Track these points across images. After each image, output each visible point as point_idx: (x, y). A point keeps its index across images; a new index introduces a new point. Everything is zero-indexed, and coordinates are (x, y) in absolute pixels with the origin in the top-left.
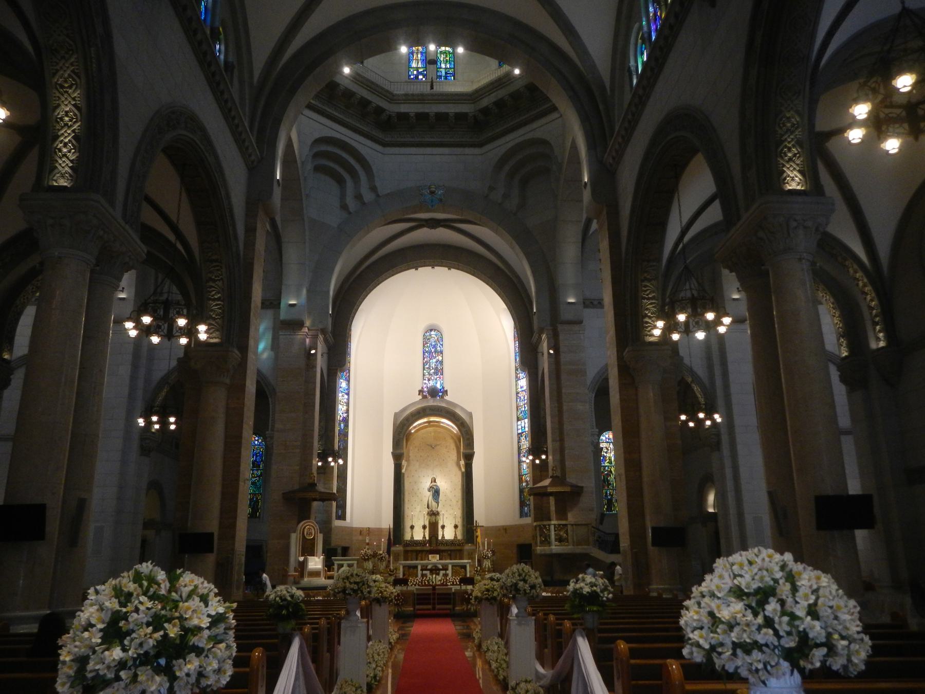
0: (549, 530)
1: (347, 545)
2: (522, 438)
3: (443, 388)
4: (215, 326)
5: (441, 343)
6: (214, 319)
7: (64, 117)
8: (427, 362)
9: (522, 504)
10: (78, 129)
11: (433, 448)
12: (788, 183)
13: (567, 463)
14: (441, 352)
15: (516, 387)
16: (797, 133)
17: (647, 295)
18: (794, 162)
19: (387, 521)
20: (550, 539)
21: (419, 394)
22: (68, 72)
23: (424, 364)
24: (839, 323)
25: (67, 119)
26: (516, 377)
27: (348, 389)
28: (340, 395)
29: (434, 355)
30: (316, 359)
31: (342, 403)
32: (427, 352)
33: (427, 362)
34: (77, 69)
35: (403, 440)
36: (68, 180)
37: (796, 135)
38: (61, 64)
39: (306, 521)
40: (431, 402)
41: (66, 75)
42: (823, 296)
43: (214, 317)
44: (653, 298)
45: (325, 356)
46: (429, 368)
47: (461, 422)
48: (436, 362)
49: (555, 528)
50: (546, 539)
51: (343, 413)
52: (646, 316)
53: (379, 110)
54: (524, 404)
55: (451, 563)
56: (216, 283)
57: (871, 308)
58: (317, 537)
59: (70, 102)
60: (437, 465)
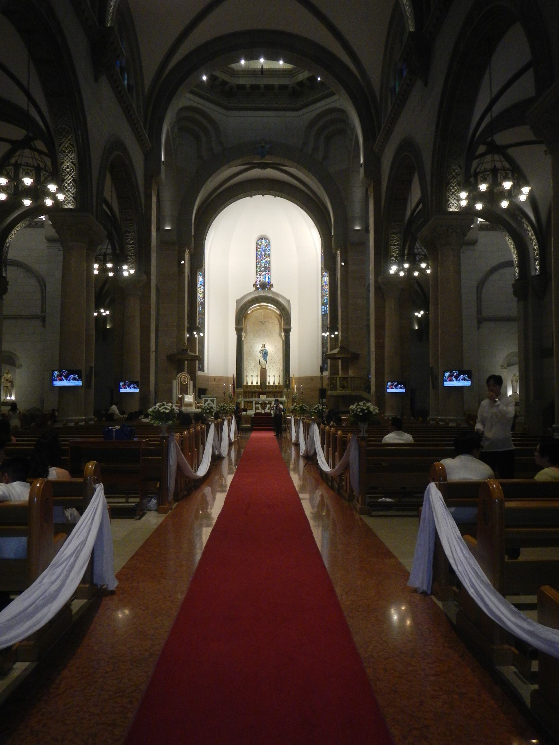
0: (336, 381)
1: (206, 388)
3: (271, 282)
4: (131, 260)
5: (269, 248)
6: (131, 256)
7: (67, 169)
8: (259, 262)
9: (324, 362)
10: (75, 176)
11: (263, 324)
12: (450, 207)
14: (269, 255)
15: (322, 282)
16: (458, 178)
17: (394, 243)
18: (455, 195)
19: (232, 372)
20: (337, 386)
21: (254, 287)
22: (68, 144)
23: (257, 264)
24: (516, 258)
25: (68, 170)
27: (204, 282)
28: (199, 286)
29: (264, 257)
30: (185, 267)
31: (200, 292)
34: (72, 142)
35: (243, 319)
36: (72, 204)
37: (458, 179)
38: (63, 140)
39: (181, 373)
40: (262, 293)
41: (66, 146)
42: (508, 240)
43: (131, 255)
44: (397, 245)
45: (189, 261)
46: (260, 267)
48: (266, 262)
49: (340, 380)
50: (334, 387)
51: (200, 299)
52: (393, 256)
53: (224, 83)
54: (327, 294)
56: (131, 233)
57: (534, 250)
58: (189, 383)
59: (69, 160)
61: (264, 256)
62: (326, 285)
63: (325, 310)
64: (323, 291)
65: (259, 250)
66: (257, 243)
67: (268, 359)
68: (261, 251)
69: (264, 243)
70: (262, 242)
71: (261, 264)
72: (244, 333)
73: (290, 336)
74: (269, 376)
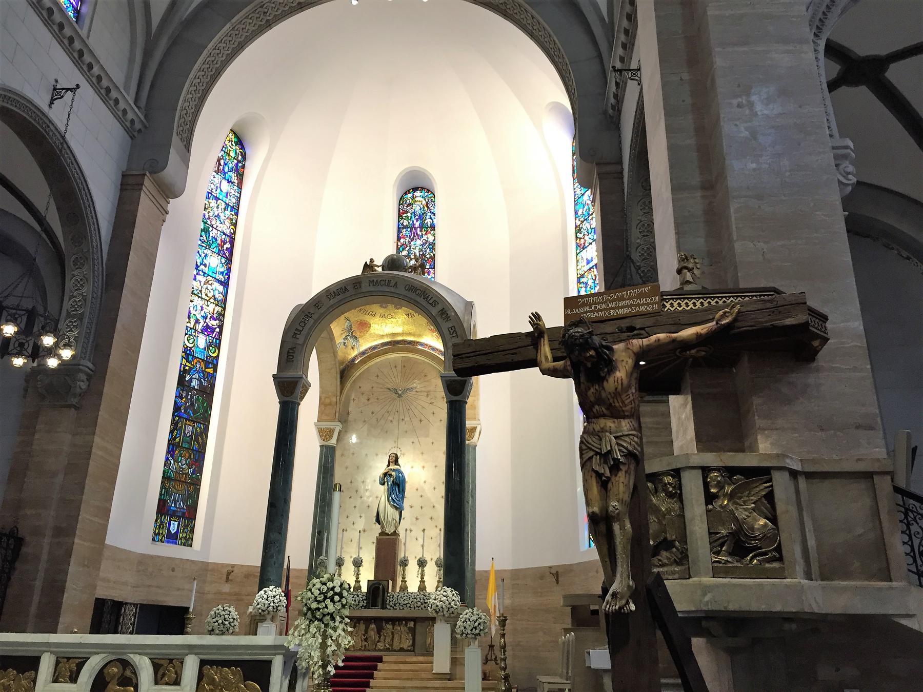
0: (677, 495)
8: (404, 246)
11: (400, 396)
13: (738, 247)
14: (433, 227)
20: (684, 539)
23: (398, 248)
26: (578, 245)
29: (419, 233)
32: (405, 227)
33: (404, 246)
47: (440, 307)
48: (423, 245)
49: (706, 486)
51: (205, 318)
55: (191, 649)
60: (406, 432)
61: (419, 229)
62: (592, 267)
66: (401, 199)
68: (411, 217)
69: (420, 199)
70: (416, 197)
71: (410, 246)
72: (339, 423)
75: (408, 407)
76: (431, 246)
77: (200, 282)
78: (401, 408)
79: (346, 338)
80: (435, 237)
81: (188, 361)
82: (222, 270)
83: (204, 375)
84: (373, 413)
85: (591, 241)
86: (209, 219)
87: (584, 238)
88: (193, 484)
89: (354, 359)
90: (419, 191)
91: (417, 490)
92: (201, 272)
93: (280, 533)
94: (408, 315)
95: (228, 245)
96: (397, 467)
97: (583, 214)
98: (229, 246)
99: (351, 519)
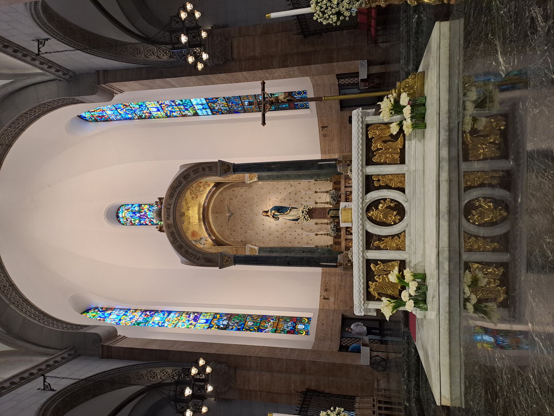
2: (217, 108)
8: (151, 221)
11: (232, 214)
14: (140, 206)
21: (164, 232)
23: (152, 225)
26: (149, 118)
32: (140, 221)
33: (151, 221)
47: (182, 179)
48: (150, 211)
51: (189, 321)
54: (176, 105)
61: (141, 214)
62: (161, 107)
63: (203, 108)
64: (175, 114)
65: (134, 221)
66: (123, 225)
67: (290, 205)
68: (134, 218)
69: (124, 213)
70: (122, 216)
71: (151, 218)
72: (247, 245)
73: (236, 163)
74: (316, 203)
75: (238, 209)
76: (151, 207)
77: (168, 324)
78: (238, 213)
79: (201, 244)
80: (145, 204)
81: (213, 327)
82: (162, 314)
83: (221, 319)
84: (241, 228)
85: (146, 109)
86: (132, 323)
87: (145, 113)
88: (279, 320)
89: (213, 240)
90: (119, 215)
91: (281, 202)
92: (163, 325)
93: (303, 258)
94: (188, 210)
95: (148, 313)
96: (269, 211)
97: (131, 114)
98: (148, 312)
99: (297, 236)
